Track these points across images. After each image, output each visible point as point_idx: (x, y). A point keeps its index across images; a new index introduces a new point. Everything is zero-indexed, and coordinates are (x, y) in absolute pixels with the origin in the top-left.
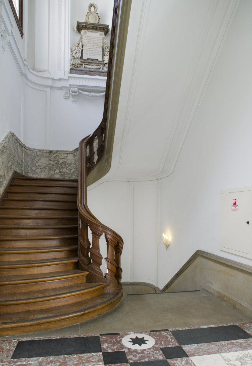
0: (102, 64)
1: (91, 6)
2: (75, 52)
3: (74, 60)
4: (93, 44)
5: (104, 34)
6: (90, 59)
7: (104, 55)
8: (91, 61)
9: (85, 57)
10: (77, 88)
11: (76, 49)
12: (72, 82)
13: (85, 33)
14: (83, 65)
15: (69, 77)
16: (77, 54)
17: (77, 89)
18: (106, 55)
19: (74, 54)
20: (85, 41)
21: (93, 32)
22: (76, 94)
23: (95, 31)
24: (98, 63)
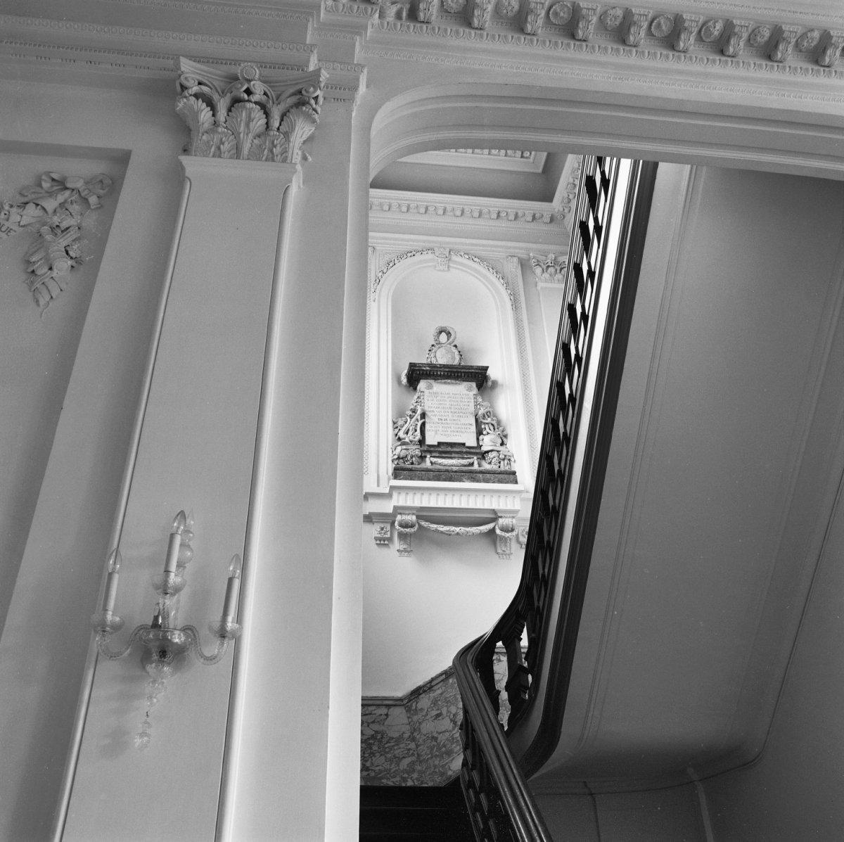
1: (441, 332)
3: (404, 447)
4: (450, 408)
5: (477, 386)
7: (479, 433)
8: (446, 449)
9: (431, 439)
10: (413, 514)
11: (406, 423)
12: (400, 500)
13: (430, 387)
14: (427, 459)
15: (392, 488)
16: (410, 433)
17: (414, 518)
18: (484, 433)
19: (401, 434)
21: (449, 383)
22: (412, 530)
23: (453, 381)
24: (467, 453)
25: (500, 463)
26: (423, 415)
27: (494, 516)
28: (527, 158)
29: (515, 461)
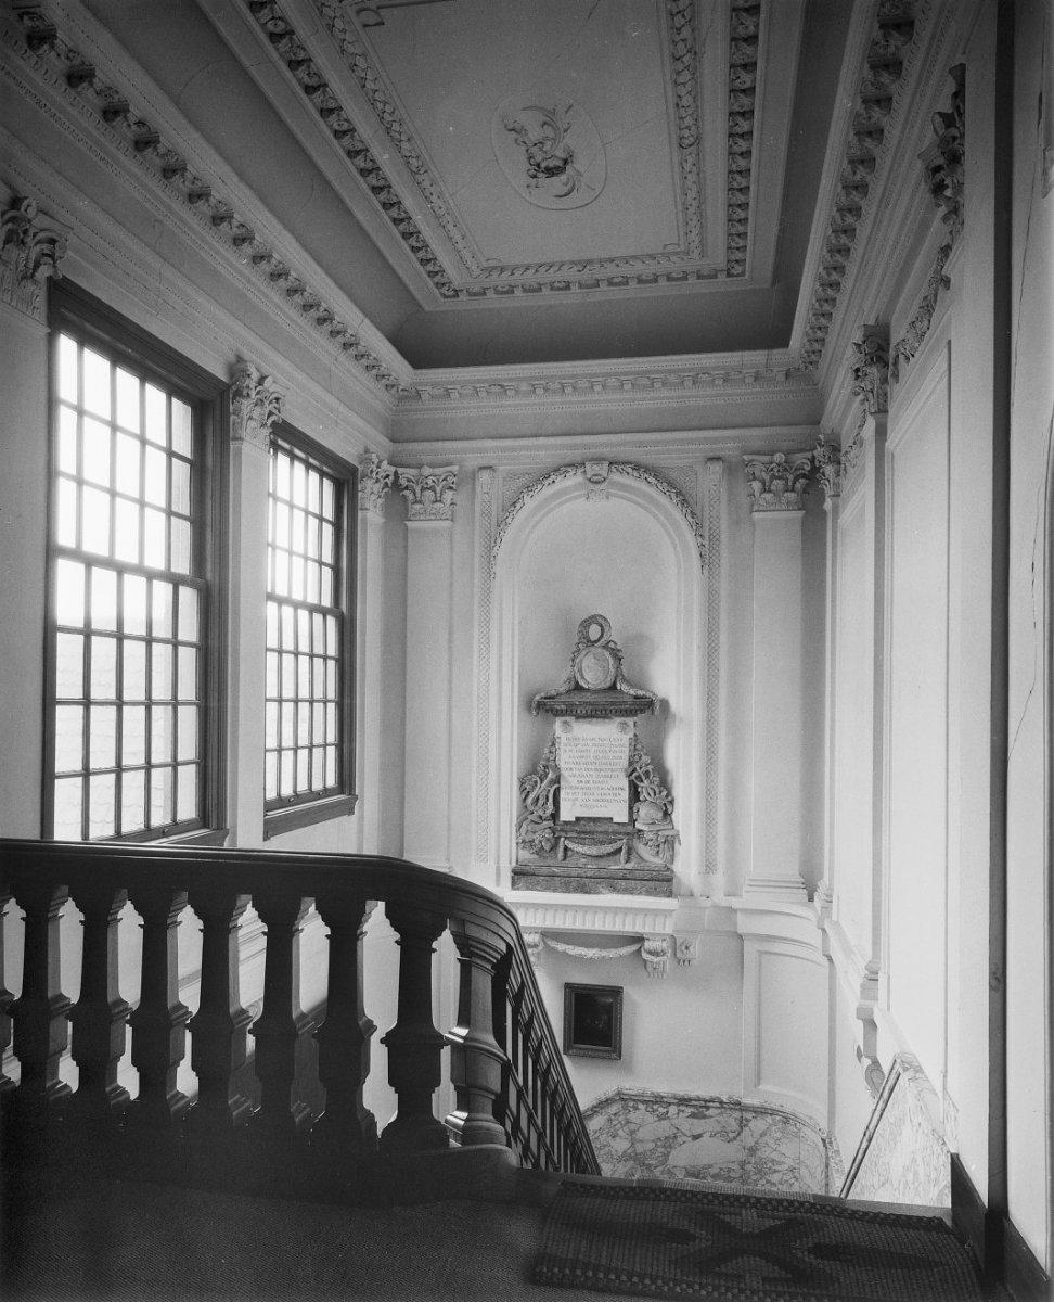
0: (628, 834)
6: (583, 818)
7: (635, 796)
8: (586, 827)
9: (567, 814)
16: (541, 802)
20: (565, 759)
25: (658, 846)
26: (557, 780)
27: (638, 939)
28: (738, 275)
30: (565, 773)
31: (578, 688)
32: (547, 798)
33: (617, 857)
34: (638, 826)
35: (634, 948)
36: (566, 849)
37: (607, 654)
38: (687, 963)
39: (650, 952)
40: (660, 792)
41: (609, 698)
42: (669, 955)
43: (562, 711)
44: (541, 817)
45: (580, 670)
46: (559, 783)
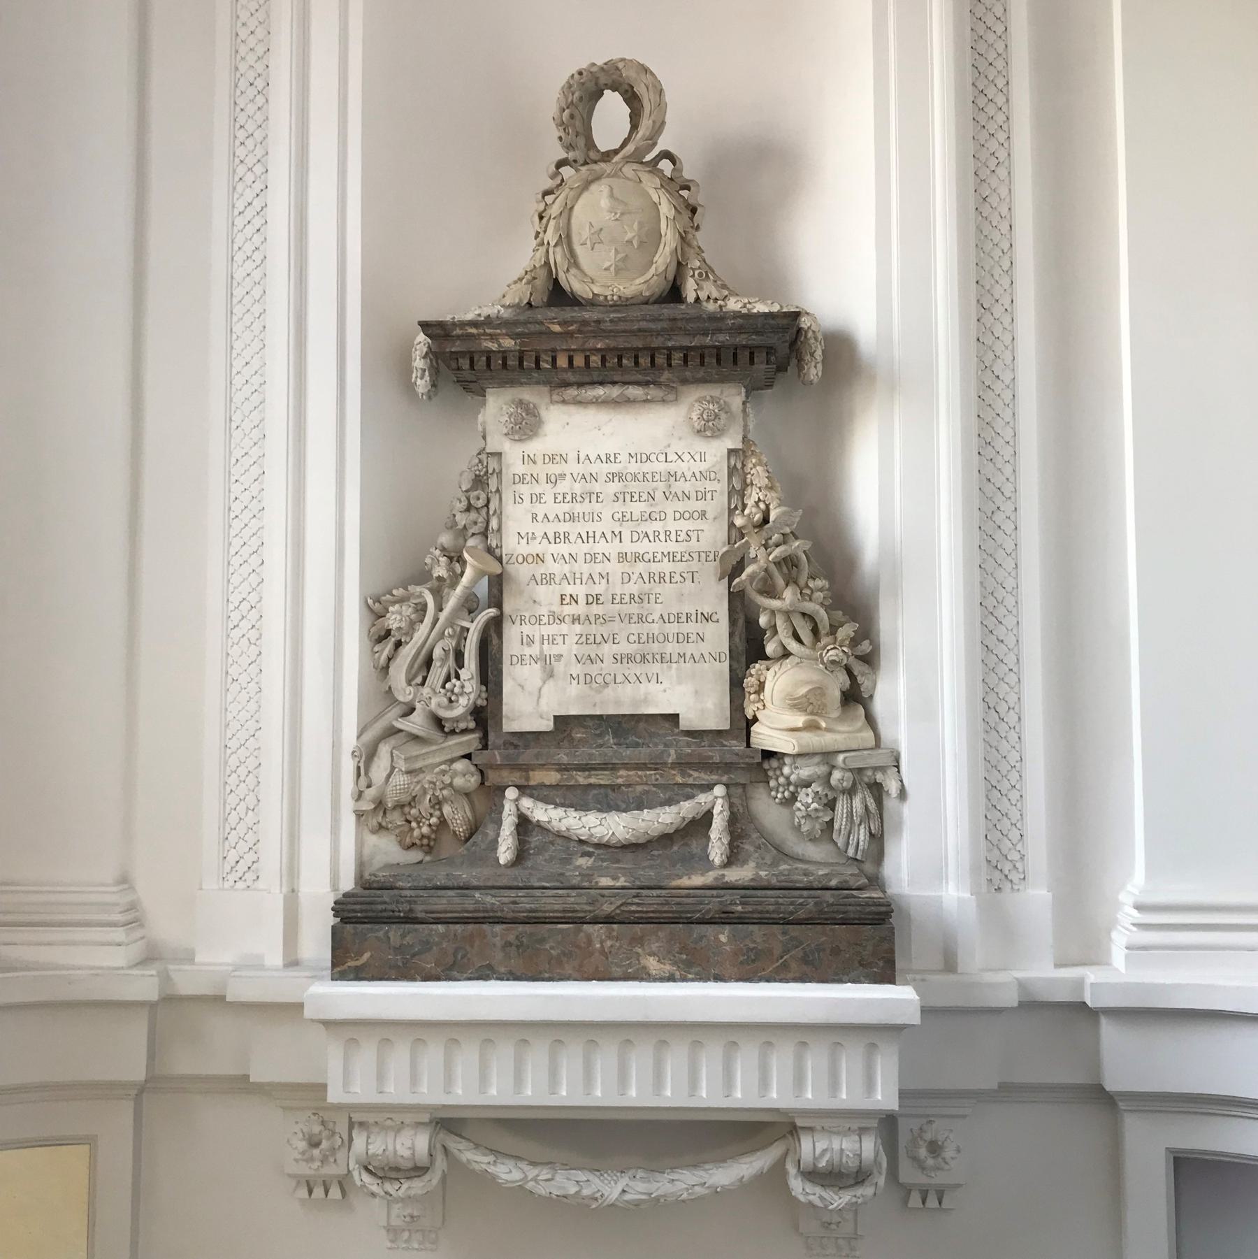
0: (727, 767)
2: (408, 652)
16: (437, 673)
18: (770, 648)
25: (831, 805)
29: (903, 794)
30: (522, 572)
31: (558, 295)
32: (459, 657)
33: (695, 846)
34: (767, 735)
35: (774, 1152)
36: (524, 824)
37: (650, 184)
38: (932, 1202)
39: (812, 1175)
40: (833, 630)
41: (668, 310)
42: (882, 1181)
43: (504, 355)
44: (438, 722)
45: (566, 239)
46: (499, 605)
